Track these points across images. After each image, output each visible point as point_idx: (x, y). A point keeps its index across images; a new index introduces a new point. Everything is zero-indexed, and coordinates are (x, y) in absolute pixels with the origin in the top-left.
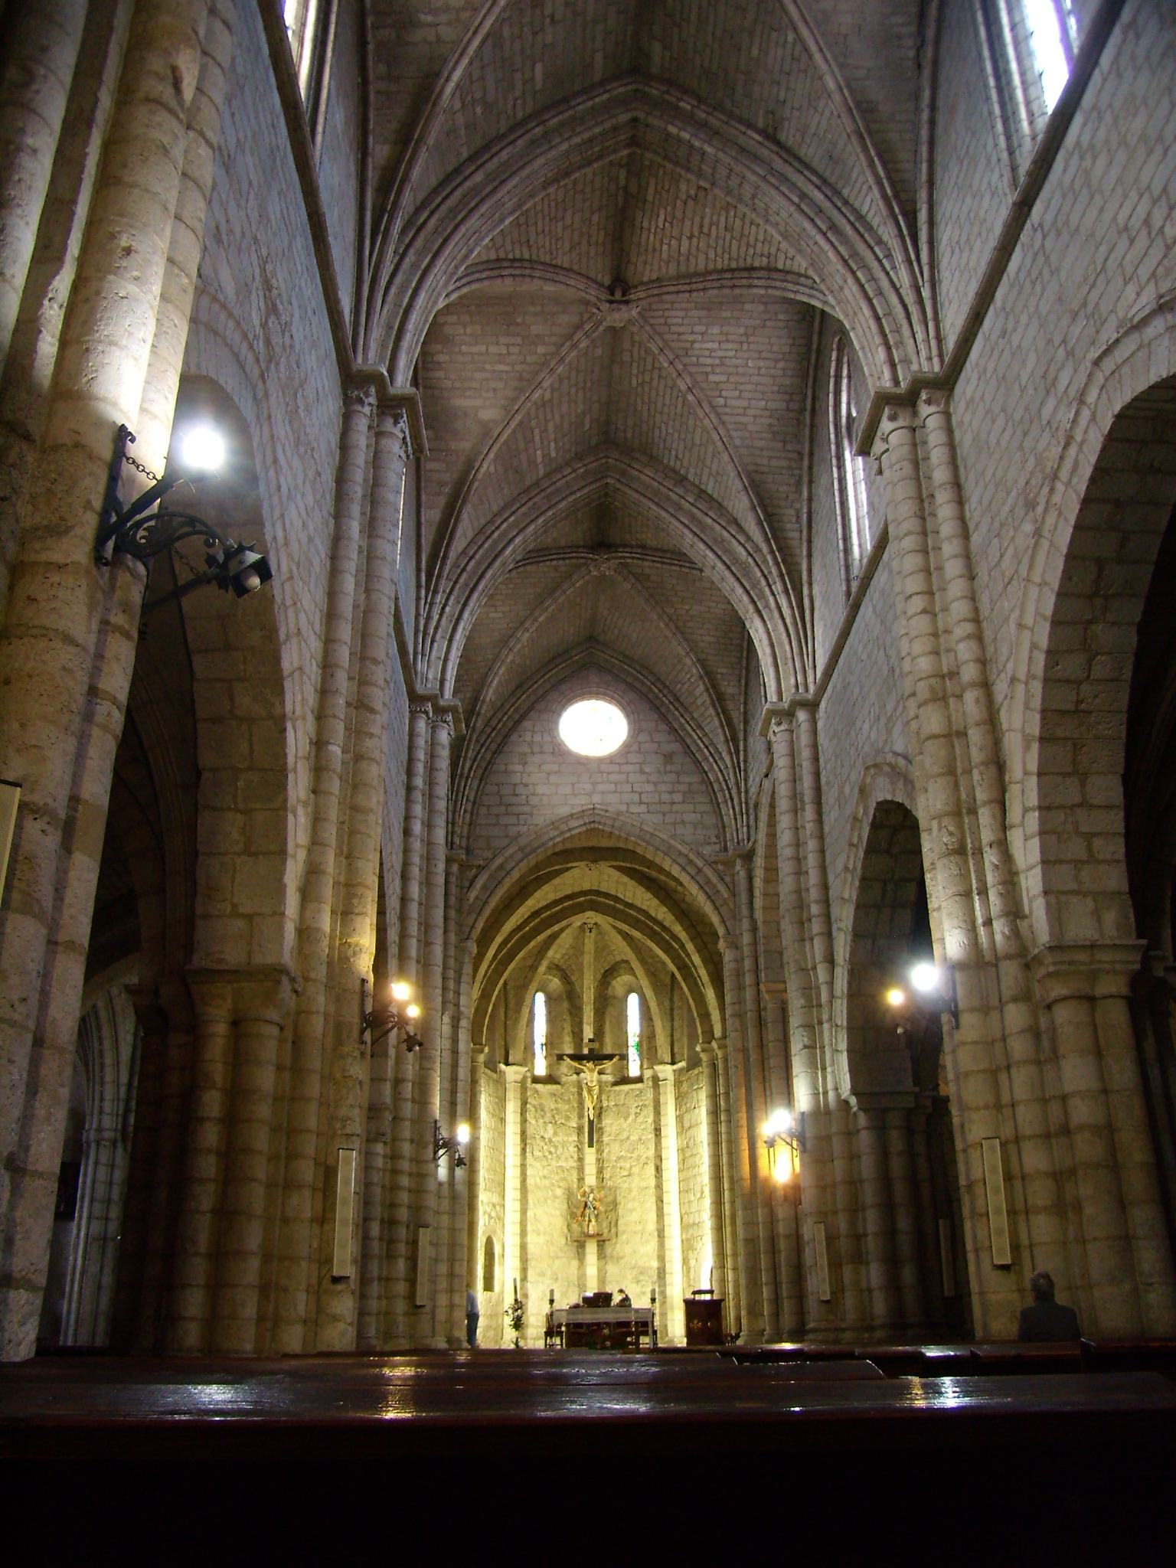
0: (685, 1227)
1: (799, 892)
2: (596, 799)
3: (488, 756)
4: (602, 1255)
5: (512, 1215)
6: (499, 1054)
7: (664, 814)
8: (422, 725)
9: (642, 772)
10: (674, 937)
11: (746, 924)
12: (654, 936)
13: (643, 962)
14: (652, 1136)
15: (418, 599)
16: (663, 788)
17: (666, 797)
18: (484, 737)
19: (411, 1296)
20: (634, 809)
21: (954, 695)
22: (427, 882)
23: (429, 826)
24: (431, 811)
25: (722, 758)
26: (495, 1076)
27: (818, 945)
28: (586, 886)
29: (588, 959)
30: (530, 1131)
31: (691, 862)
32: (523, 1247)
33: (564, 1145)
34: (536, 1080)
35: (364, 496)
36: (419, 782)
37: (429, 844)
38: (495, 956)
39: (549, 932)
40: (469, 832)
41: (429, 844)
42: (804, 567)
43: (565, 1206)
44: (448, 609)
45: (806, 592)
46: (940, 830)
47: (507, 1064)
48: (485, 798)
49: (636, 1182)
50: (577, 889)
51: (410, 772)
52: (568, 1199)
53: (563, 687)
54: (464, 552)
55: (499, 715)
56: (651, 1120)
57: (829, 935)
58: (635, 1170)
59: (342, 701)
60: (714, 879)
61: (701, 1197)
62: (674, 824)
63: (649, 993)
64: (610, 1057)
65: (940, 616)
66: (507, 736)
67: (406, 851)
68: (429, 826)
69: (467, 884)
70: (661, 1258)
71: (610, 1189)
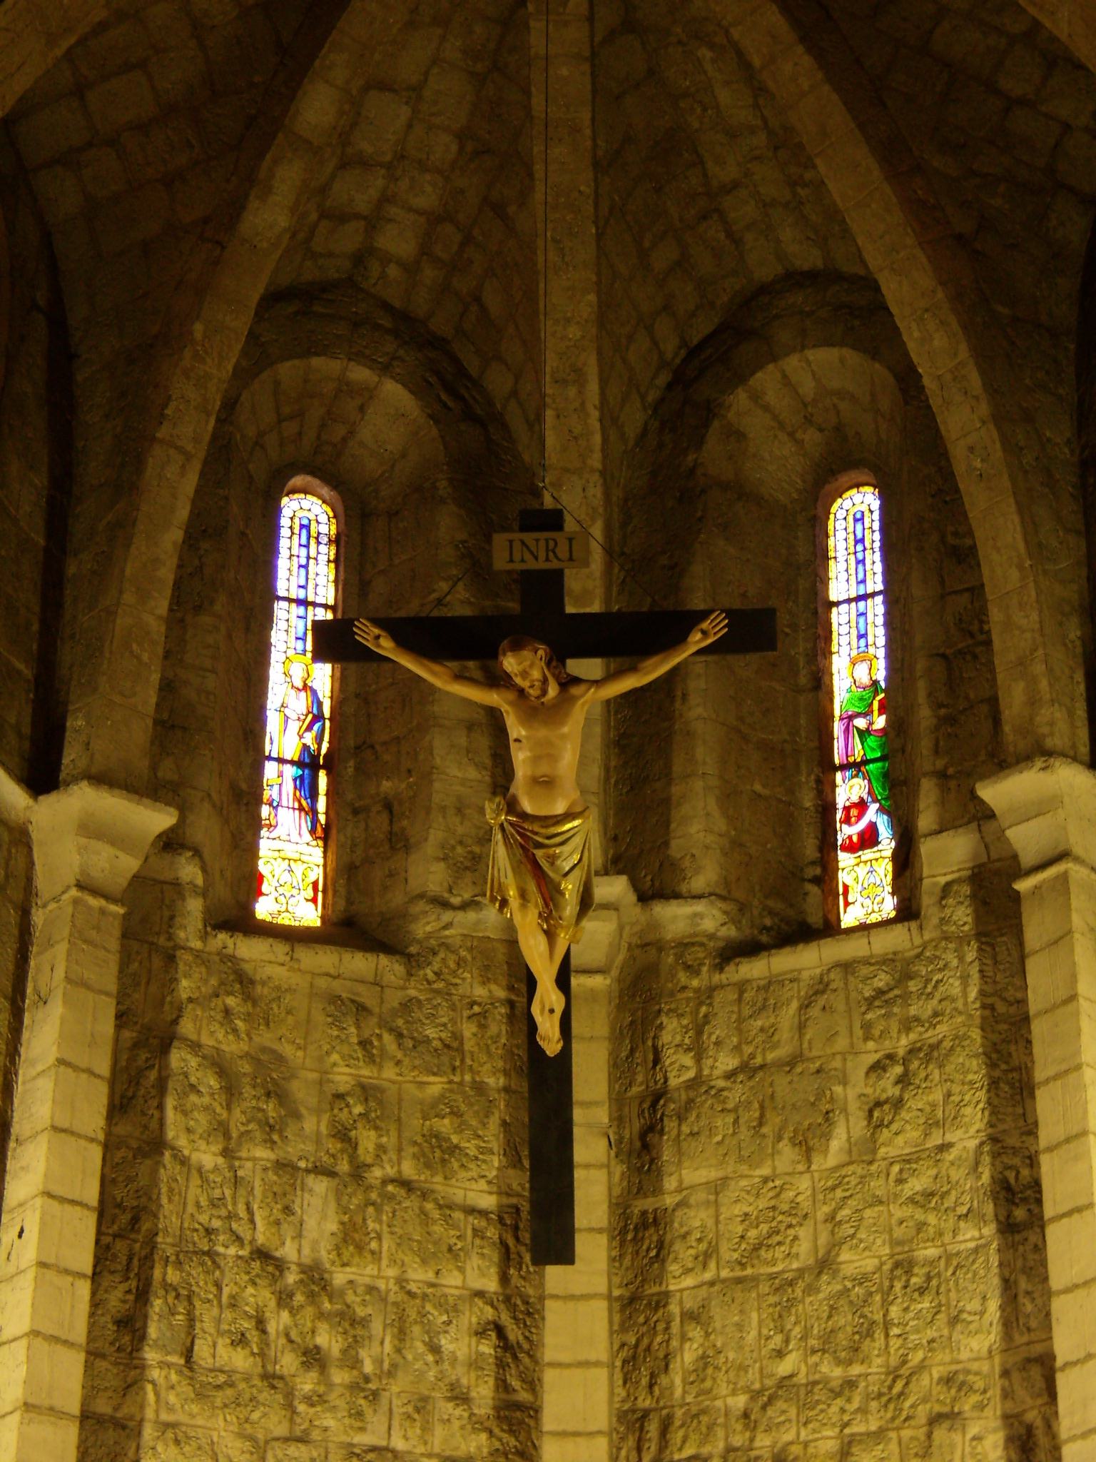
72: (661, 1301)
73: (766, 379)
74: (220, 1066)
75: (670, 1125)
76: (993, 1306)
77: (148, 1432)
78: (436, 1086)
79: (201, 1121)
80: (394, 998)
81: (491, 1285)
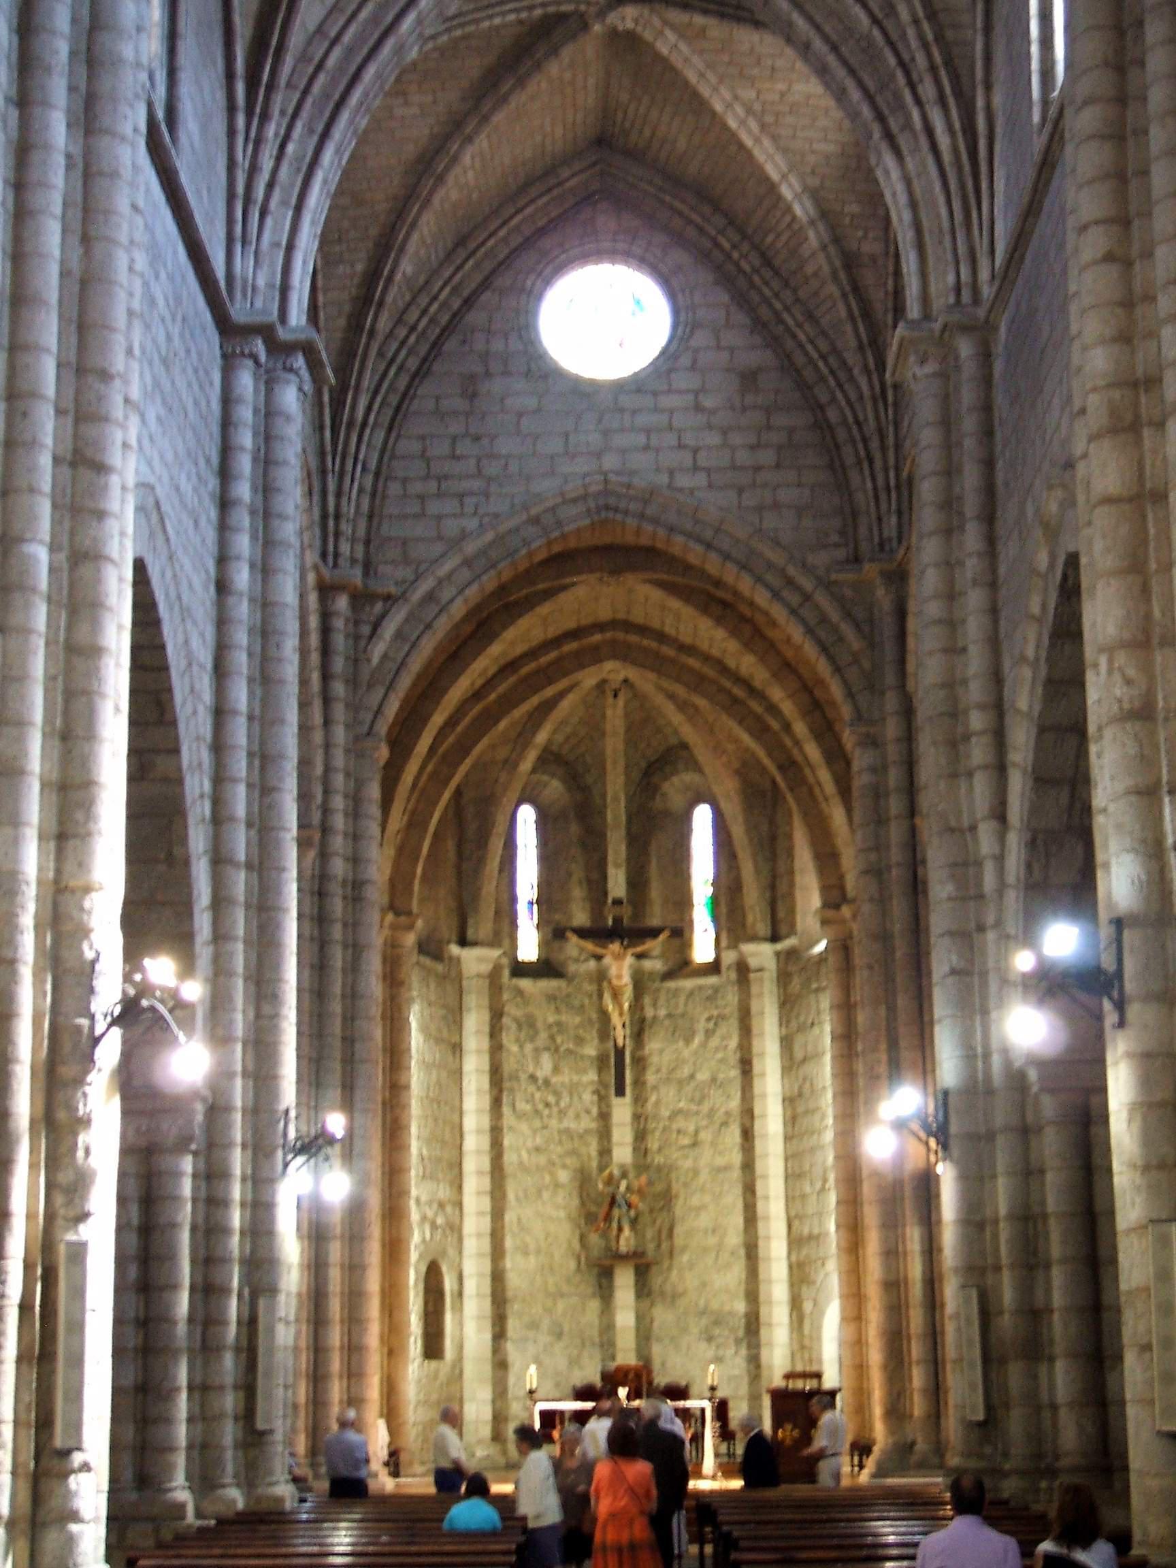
0: (796, 1241)
1: (952, 684)
2: (610, 462)
3: (403, 383)
4: (643, 1290)
5: (475, 1222)
6: (447, 928)
7: (741, 491)
8: (246, 381)
9: (698, 408)
10: (773, 709)
11: (891, 702)
12: (733, 706)
13: (718, 749)
14: (735, 1073)
15: (231, 132)
16: (737, 439)
17: (743, 457)
18: (394, 346)
19: (248, 1415)
20: (683, 481)
21: (1151, 423)
22: (265, 678)
23: (265, 570)
24: (267, 543)
25: (852, 379)
26: (440, 968)
27: (981, 787)
28: (604, 614)
29: (614, 746)
30: (509, 1065)
31: (790, 582)
32: (498, 1278)
33: (573, 1089)
34: (520, 970)
35: (73, 54)
36: (243, 490)
37: (265, 604)
38: (432, 749)
39: (535, 700)
40: (368, 533)
41: (265, 604)
42: (979, 46)
43: (576, 1202)
44: (291, 148)
45: (980, 103)
46: (1110, 671)
47: (463, 942)
48: (395, 463)
49: (706, 1157)
50: (586, 621)
51: (225, 473)
52: (581, 1187)
53: (546, 243)
54: (320, 30)
55: (423, 300)
56: (733, 1043)
57: (1000, 768)
58: (705, 1136)
59: (45, 461)
60: (834, 615)
61: (823, 1189)
62: (760, 509)
63: (733, 809)
64: (654, 933)
65: (1137, 267)
66: (436, 345)
67: (222, 622)
68: (265, 570)
69: (366, 630)
70: (753, 1295)
71: (659, 1169)
72: (644, 1083)
73: (675, 780)
74: (516, 1020)
75: (647, 1029)
76: (739, 1094)
77: (505, 1130)
78: (577, 1020)
79: (512, 1037)
80: (564, 993)
81: (596, 1078)
